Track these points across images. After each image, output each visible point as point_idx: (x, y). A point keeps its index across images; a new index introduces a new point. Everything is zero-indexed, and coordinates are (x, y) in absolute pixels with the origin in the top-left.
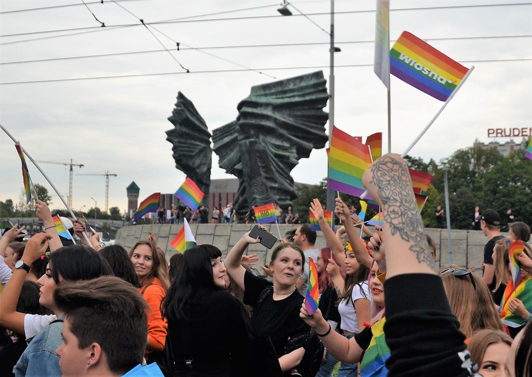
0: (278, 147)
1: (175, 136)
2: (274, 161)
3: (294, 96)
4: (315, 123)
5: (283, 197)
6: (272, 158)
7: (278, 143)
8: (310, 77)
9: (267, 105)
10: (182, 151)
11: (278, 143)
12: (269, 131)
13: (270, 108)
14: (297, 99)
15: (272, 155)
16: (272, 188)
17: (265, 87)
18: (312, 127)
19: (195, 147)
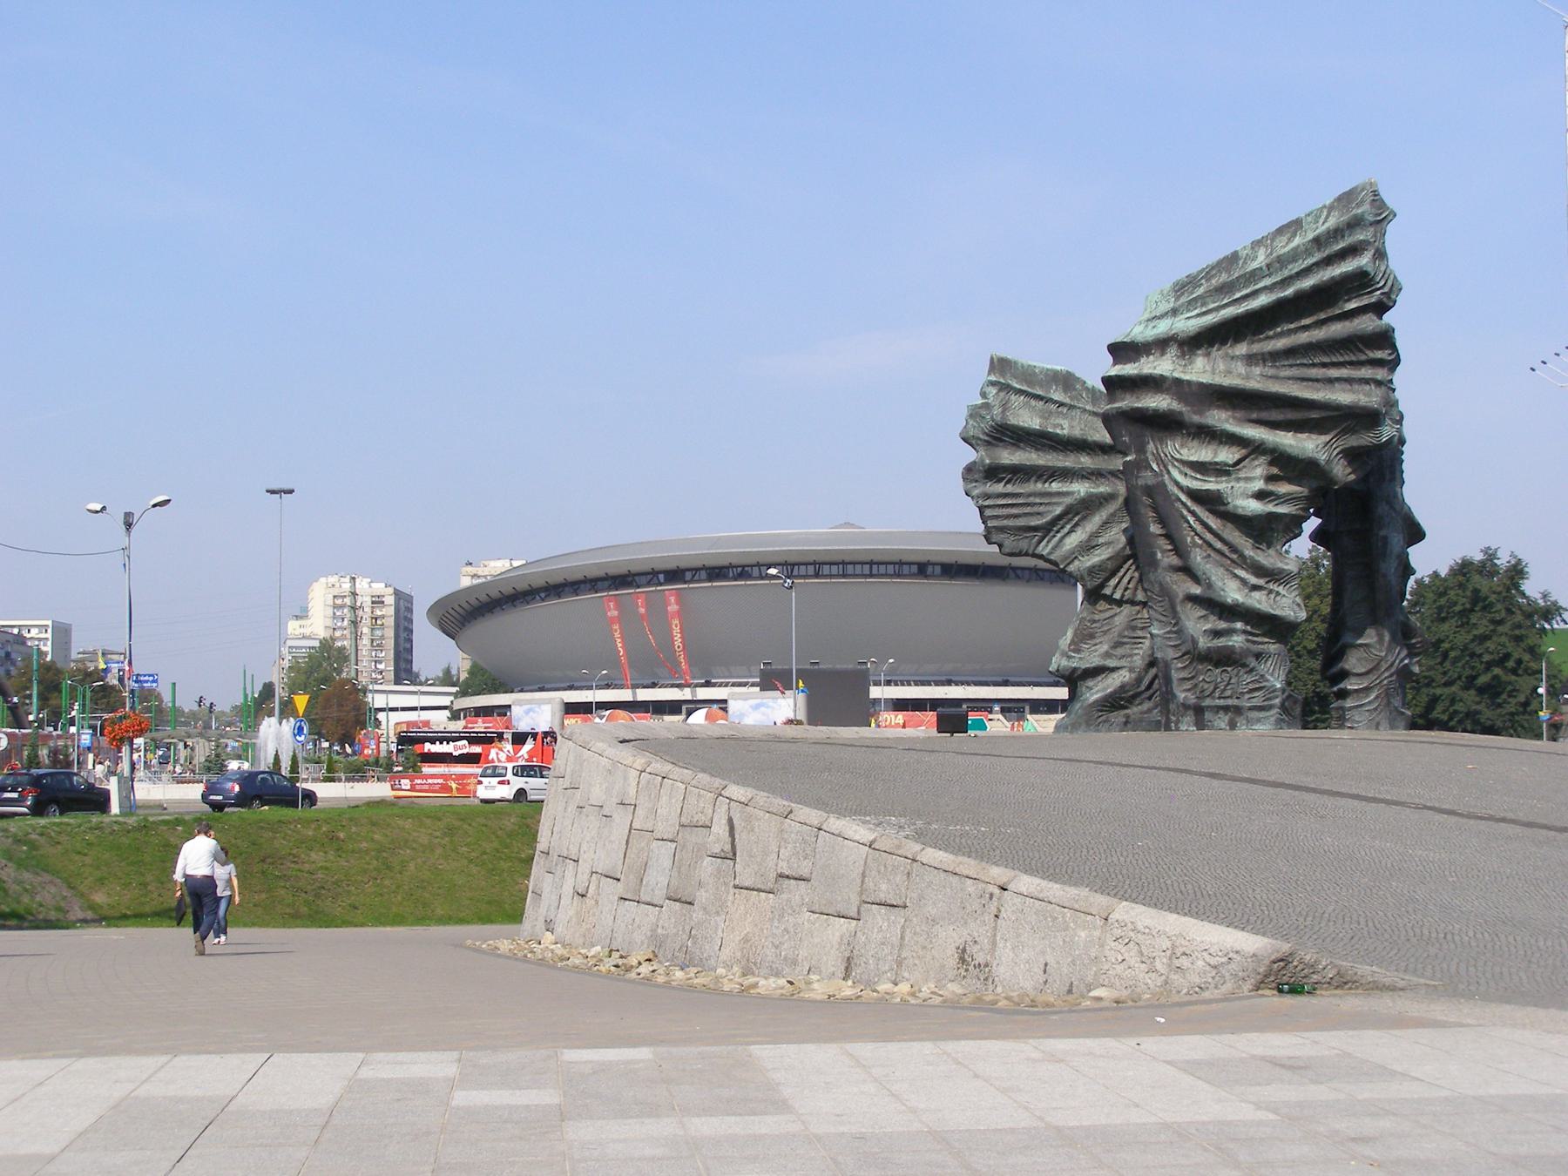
0: (1201, 468)
2: (1193, 513)
3: (1255, 294)
4: (1351, 363)
5: (1223, 625)
6: (1184, 504)
8: (1325, 213)
9: (1162, 344)
10: (997, 517)
11: (1204, 453)
12: (1166, 424)
13: (1173, 351)
14: (1263, 300)
15: (1183, 498)
17: (1180, 288)
19: (1054, 500)
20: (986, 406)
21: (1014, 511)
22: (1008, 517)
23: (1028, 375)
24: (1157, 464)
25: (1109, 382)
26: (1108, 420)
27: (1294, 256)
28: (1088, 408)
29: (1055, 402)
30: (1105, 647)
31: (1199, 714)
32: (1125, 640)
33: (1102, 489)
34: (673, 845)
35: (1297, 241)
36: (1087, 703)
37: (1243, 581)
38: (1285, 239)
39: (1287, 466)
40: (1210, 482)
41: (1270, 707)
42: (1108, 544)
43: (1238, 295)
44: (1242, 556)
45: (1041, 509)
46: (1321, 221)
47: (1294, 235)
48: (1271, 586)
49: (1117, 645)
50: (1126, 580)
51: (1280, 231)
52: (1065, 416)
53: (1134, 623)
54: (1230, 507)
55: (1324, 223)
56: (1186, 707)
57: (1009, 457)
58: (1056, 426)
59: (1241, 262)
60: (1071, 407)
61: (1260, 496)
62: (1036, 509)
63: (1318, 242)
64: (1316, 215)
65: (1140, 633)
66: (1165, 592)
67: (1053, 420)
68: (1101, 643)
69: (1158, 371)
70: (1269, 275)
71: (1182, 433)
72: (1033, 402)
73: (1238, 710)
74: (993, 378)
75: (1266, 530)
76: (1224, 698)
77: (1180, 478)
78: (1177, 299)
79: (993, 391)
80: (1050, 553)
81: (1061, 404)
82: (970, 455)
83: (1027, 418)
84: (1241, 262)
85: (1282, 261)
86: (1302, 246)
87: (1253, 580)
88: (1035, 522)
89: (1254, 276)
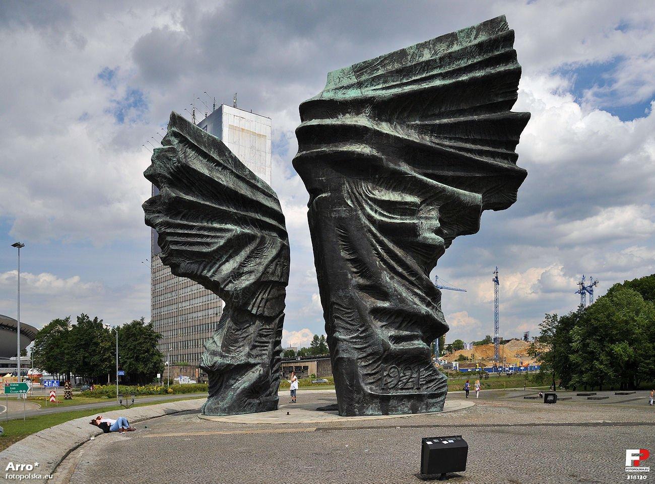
1: (159, 212)
2: (381, 243)
8: (475, 32)
10: (176, 243)
14: (438, 83)
16: (378, 313)
22: (185, 244)
24: (352, 201)
32: (257, 344)
35: (456, 48)
40: (396, 219)
45: (209, 240)
46: (472, 37)
49: (254, 347)
50: (258, 301)
51: (440, 40)
53: (260, 332)
54: (420, 238)
55: (475, 38)
58: (219, 178)
59: (409, 57)
62: (204, 240)
63: (480, 46)
64: (468, 32)
65: (264, 339)
66: (354, 304)
68: (243, 346)
70: (440, 67)
71: (375, 178)
73: (420, 398)
76: (408, 389)
80: (212, 276)
81: (218, 164)
84: (409, 57)
86: (469, 48)
88: (205, 250)
89: (428, 65)
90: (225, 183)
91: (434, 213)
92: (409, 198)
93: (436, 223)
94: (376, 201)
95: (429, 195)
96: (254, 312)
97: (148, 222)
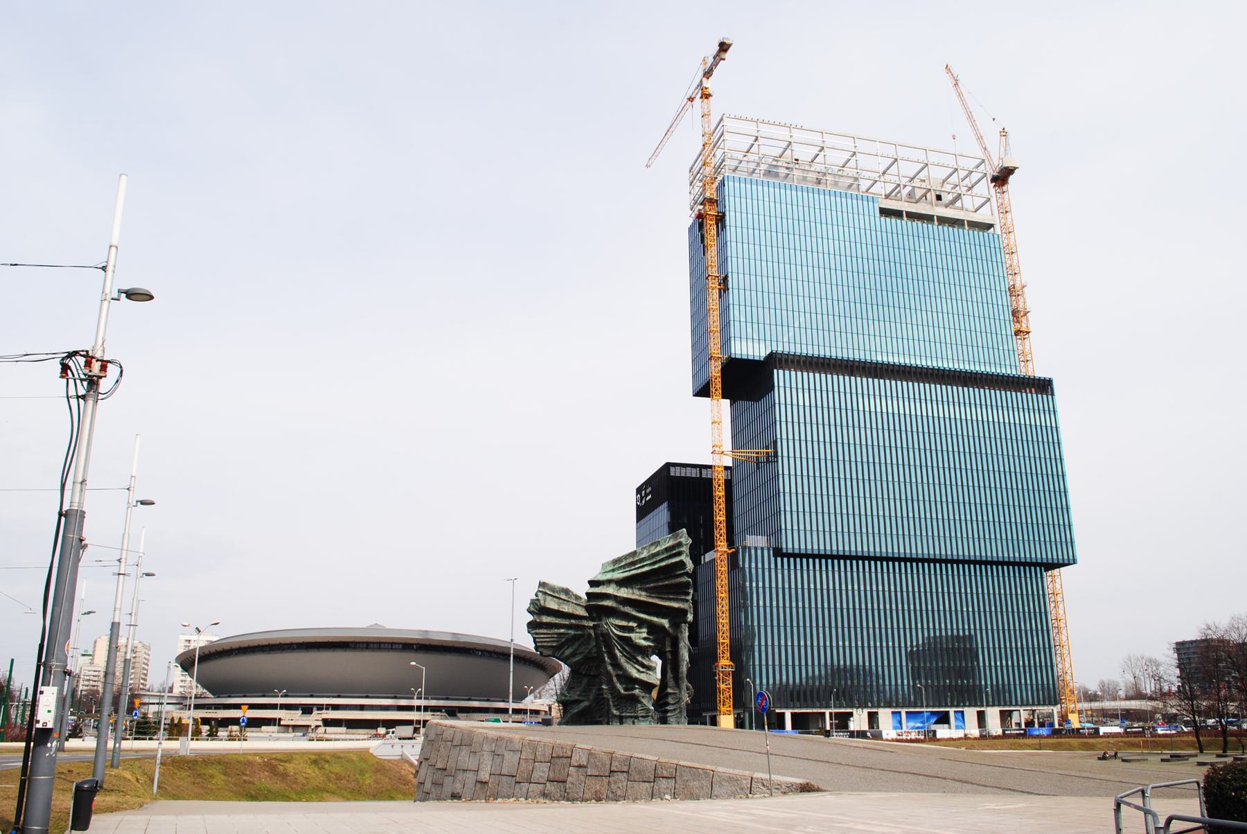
3: (643, 566)
5: (630, 686)
7: (624, 623)
9: (609, 582)
11: (624, 623)
12: (611, 612)
17: (615, 562)
18: (670, 599)
20: (538, 600)
21: (547, 640)
23: (553, 589)
25: (587, 594)
26: (587, 608)
27: (657, 554)
28: (574, 602)
29: (562, 599)
30: (578, 693)
31: (621, 720)
33: (579, 633)
34: (549, 764)
36: (572, 714)
37: (638, 670)
38: (653, 547)
39: (653, 629)
41: (648, 716)
42: (581, 653)
43: (637, 566)
44: (637, 660)
47: (657, 547)
48: (648, 672)
52: (566, 604)
56: (616, 716)
57: (546, 619)
58: (563, 608)
60: (568, 601)
61: (645, 639)
63: (667, 550)
67: (562, 606)
69: (608, 592)
72: (555, 599)
74: (540, 589)
75: (645, 652)
77: (613, 629)
78: (614, 566)
79: (540, 594)
81: (565, 600)
82: (530, 618)
83: (552, 604)
85: (654, 555)
87: (641, 669)
90: (566, 611)
91: (645, 630)
92: (631, 624)
93: (645, 635)
94: (616, 625)
95: (641, 623)
96: (584, 673)
97: (529, 632)
